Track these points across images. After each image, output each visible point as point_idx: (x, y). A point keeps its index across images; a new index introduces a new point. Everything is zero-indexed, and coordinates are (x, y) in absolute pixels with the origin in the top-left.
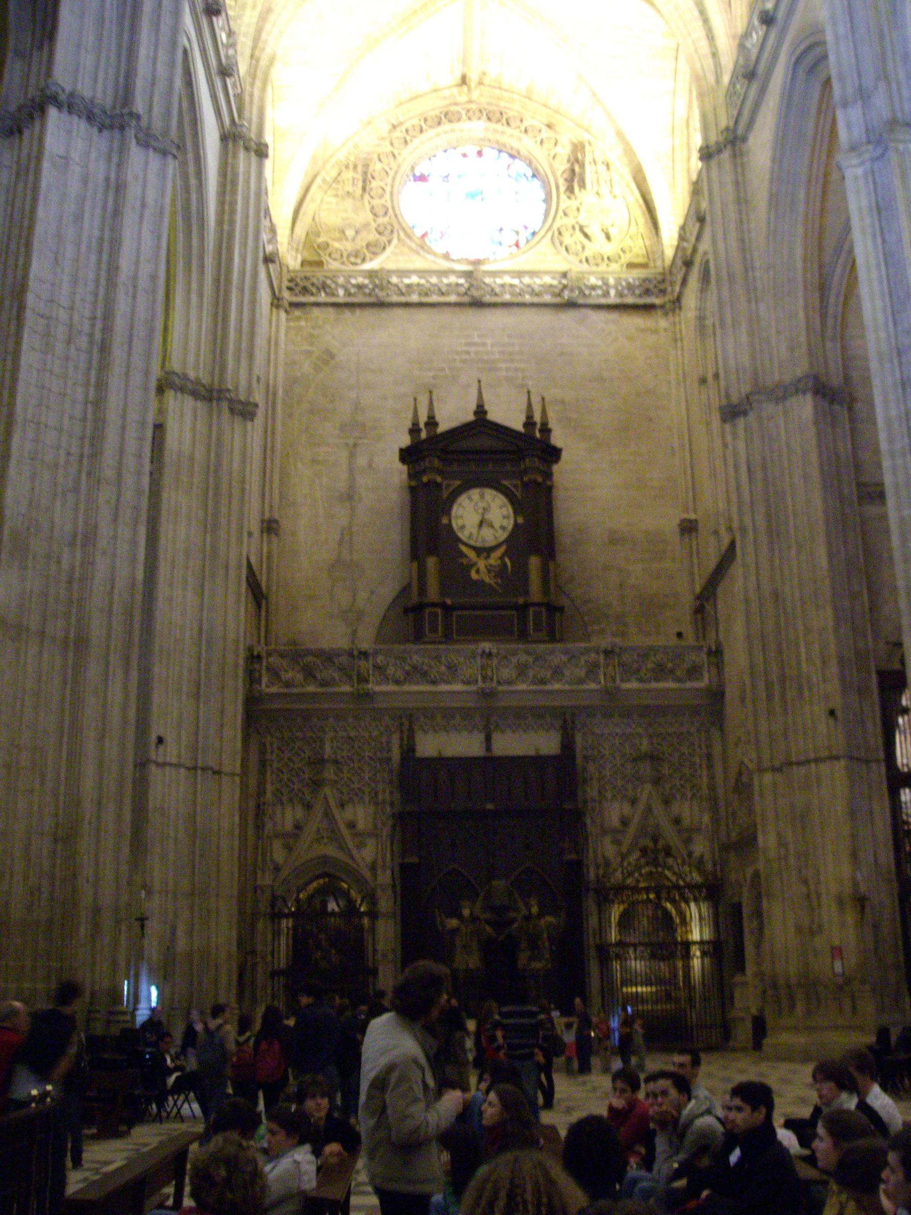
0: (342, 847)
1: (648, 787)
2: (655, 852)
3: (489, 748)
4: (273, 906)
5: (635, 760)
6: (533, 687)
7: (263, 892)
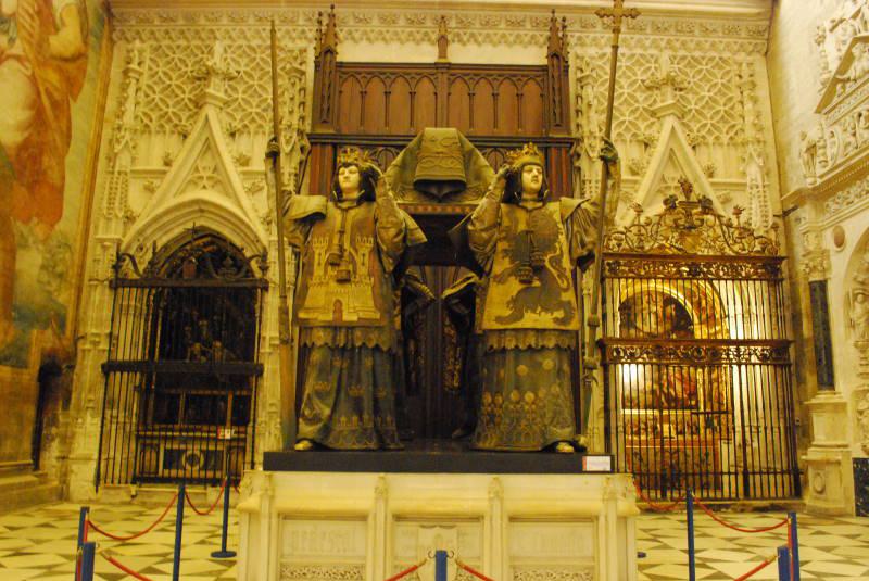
0: (228, 190)
1: (670, 122)
2: (688, 208)
3: (443, 54)
4: (116, 268)
5: (649, 88)
7: (105, 248)
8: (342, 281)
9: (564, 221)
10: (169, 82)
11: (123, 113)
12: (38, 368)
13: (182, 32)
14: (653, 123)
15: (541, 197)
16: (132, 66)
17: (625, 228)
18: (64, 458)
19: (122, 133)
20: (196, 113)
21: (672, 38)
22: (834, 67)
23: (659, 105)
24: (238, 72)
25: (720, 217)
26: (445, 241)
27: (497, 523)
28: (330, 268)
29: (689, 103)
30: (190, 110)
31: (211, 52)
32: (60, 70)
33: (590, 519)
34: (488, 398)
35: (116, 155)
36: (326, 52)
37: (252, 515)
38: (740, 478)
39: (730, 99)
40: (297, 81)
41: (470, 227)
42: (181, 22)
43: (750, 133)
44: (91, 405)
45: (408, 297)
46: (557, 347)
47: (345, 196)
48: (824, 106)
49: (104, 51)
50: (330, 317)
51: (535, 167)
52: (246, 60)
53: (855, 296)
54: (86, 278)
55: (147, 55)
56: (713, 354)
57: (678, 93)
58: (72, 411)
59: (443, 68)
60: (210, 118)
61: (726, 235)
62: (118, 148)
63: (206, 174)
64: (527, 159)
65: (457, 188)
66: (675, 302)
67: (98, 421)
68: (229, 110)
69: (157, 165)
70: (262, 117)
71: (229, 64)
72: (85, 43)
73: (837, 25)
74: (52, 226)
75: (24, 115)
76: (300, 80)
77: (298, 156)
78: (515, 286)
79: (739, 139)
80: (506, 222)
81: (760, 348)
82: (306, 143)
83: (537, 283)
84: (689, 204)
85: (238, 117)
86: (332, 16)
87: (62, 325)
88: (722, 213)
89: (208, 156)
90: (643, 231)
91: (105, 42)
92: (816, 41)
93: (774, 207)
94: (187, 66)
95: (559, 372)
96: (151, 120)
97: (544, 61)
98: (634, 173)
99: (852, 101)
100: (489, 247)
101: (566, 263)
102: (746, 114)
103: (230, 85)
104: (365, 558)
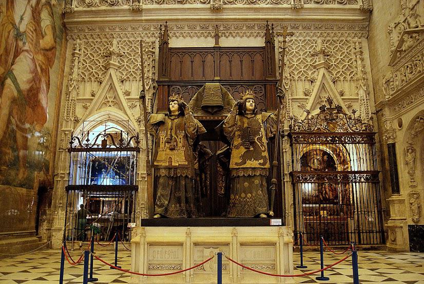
1: (322, 71)
2: (331, 111)
3: (217, 43)
5: (313, 55)
6: (246, 6)
8: (172, 149)
9: (263, 122)
10: (93, 58)
11: (73, 73)
12: (37, 189)
13: (99, 35)
14: (315, 72)
15: (254, 112)
16: (76, 51)
17: (302, 120)
18: (49, 230)
19: (73, 82)
20: (105, 72)
21: (323, 32)
22: (396, 44)
23: (317, 63)
24: (124, 53)
25: (346, 115)
26: (214, 131)
27: (235, 246)
28: (167, 144)
29: (332, 62)
30: (103, 71)
31: (112, 44)
32: (44, 55)
33: (273, 244)
34: (232, 196)
35: (70, 92)
36: (164, 43)
37: (137, 244)
38: (357, 235)
39: (351, 59)
40: (151, 57)
41: (224, 126)
42: (98, 30)
43: (360, 75)
44: (61, 205)
45: (202, 155)
46: (260, 174)
47: (172, 114)
48: (393, 63)
49: (63, 45)
50: (167, 164)
51: (251, 100)
52: (128, 47)
53: (408, 150)
54: (57, 149)
55: (83, 47)
56: (346, 177)
57: (326, 57)
58: (52, 209)
59: (217, 49)
60: (112, 73)
61: (349, 123)
62: (70, 89)
63: (110, 100)
64: (248, 96)
65: (220, 109)
66: (329, 155)
67: (64, 212)
68: (120, 70)
69: (88, 96)
70: (135, 73)
71: (120, 49)
72: (55, 42)
73: (397, 25)
74: (43, 125)
75: (30, 76)
76: (152, 56)
77: (152, 91)
78: (243, 150)
79: (355, 78)
80: (239, 123)
81: (365, 175)
82: (156, 84)
83: (252, 149)
84: (331, 109)
85: (124, 74)
86: (166, 27)
87: (47, 170)
88: (347, 113)
89: (111, 92)
90: (310, 122)
91: (63, 40)
92: (388, 32)
93: (372, 109)
94: (101, 51)
95: (262, 185)
96: (85, 76)
97: (264, 45)
98: (306, 95)
99: (403, 60)
100: (232, 134)
101: (265, 140)
102: (358, 67)
103: (121, 59)
104: (182, 261)
